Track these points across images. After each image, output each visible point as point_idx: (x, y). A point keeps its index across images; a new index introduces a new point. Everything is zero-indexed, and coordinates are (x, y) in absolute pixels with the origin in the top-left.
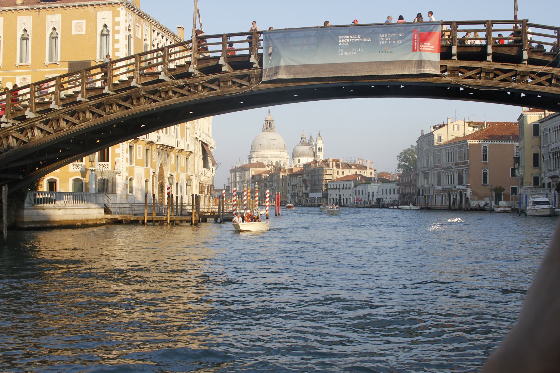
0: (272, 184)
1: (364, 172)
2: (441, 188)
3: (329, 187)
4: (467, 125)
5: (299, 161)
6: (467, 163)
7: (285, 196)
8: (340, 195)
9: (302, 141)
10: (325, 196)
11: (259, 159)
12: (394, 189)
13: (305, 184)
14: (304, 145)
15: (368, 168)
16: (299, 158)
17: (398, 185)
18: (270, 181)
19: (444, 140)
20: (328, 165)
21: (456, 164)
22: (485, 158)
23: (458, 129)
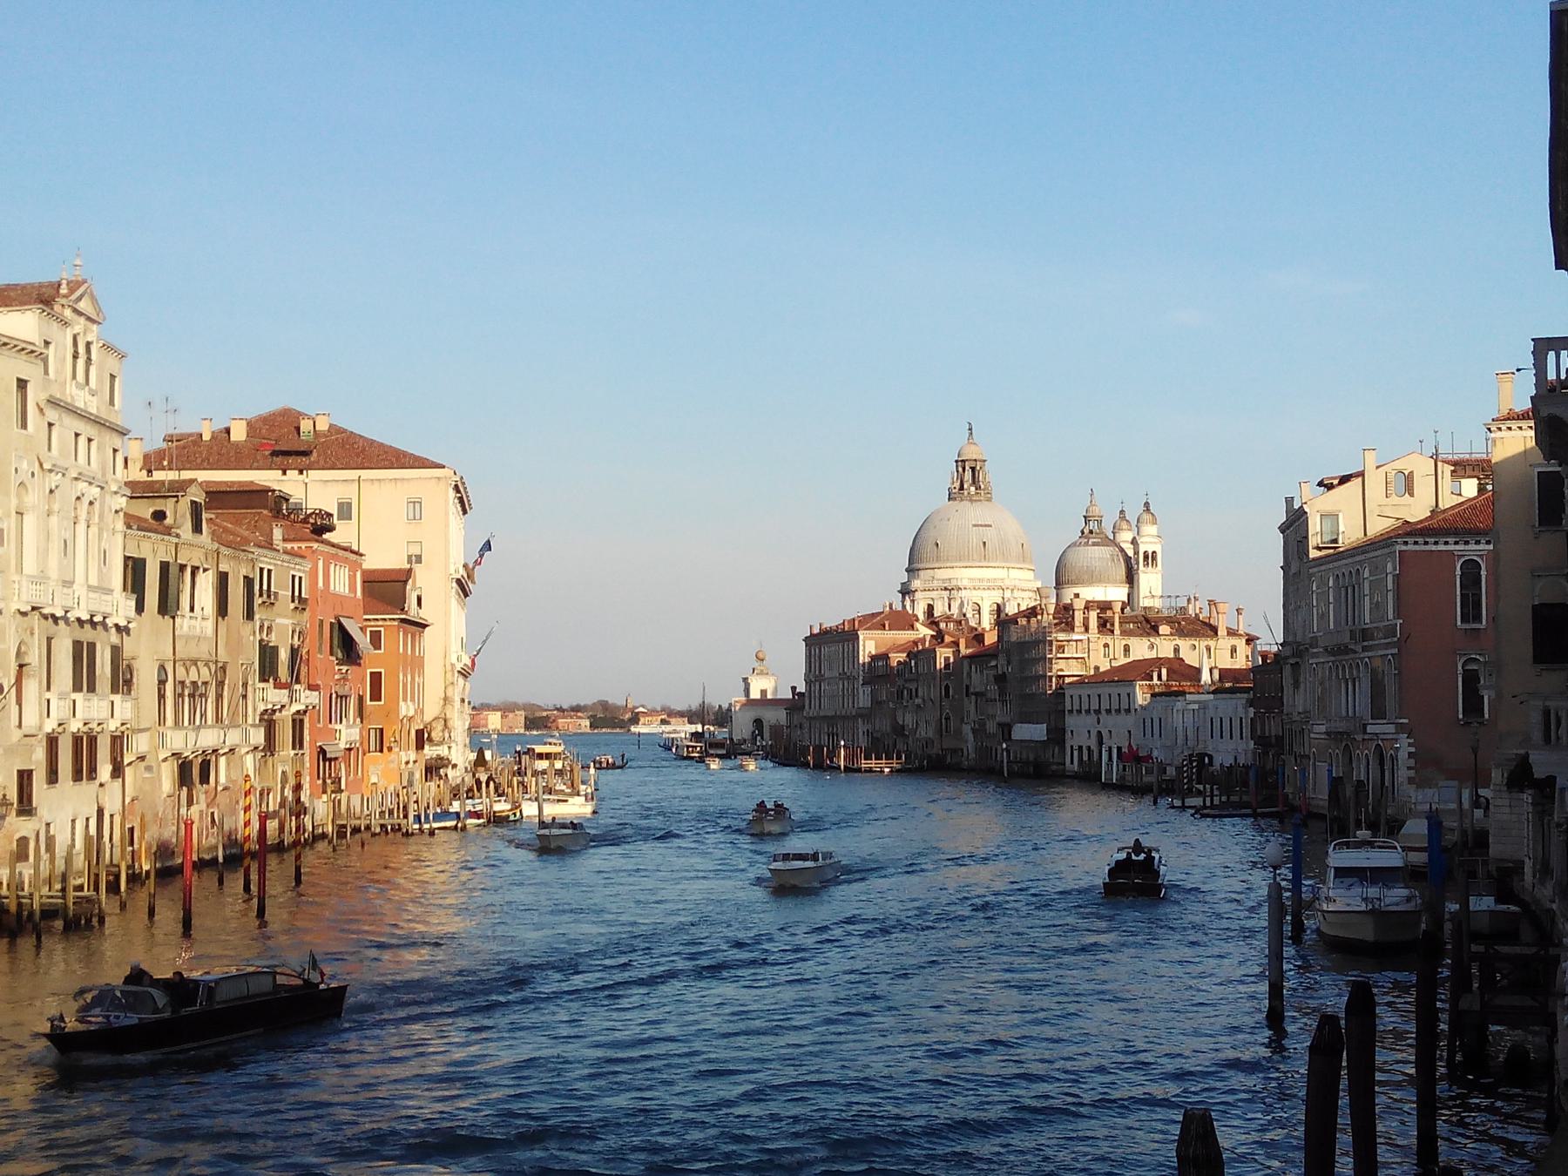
0: (917, 690)
1: (1208, 649)
2: (1323, 729)
3: (1068, 706)
4: (1448, 474)
5: (1077, 596)
6: (1390, 631)
7: (959, 732)
8: (1099, 733)
9: (1086, 531)
10: (1057, 735)
11: (934, 594)
12: (1241, 719)
13: (1002, 693)
14: (1094, 544)
15: (1219, 633)
16: (1076, 590)
17: (1251, 703)
18: (912, 676)
19: (1350, 533)
20: (1070, 627)
21: (1365, 634)
22: (1471, 609)
23: (1409, 489)
